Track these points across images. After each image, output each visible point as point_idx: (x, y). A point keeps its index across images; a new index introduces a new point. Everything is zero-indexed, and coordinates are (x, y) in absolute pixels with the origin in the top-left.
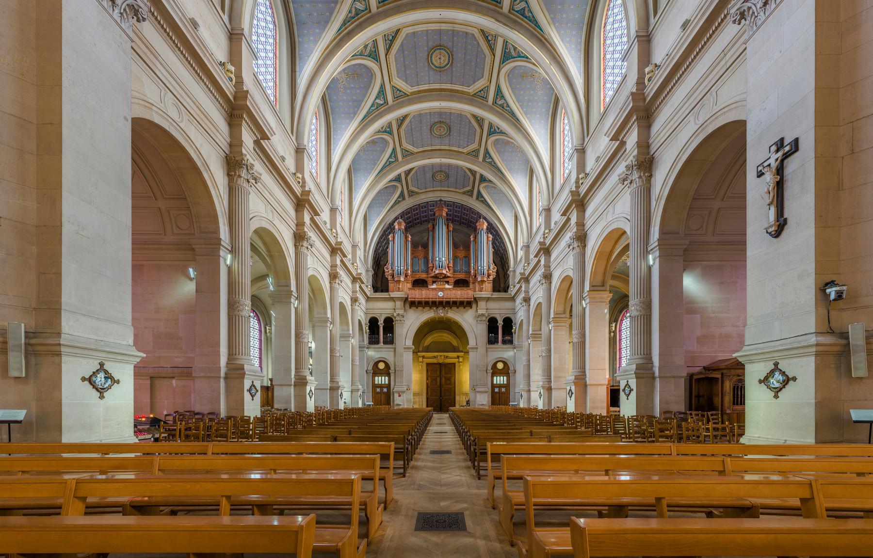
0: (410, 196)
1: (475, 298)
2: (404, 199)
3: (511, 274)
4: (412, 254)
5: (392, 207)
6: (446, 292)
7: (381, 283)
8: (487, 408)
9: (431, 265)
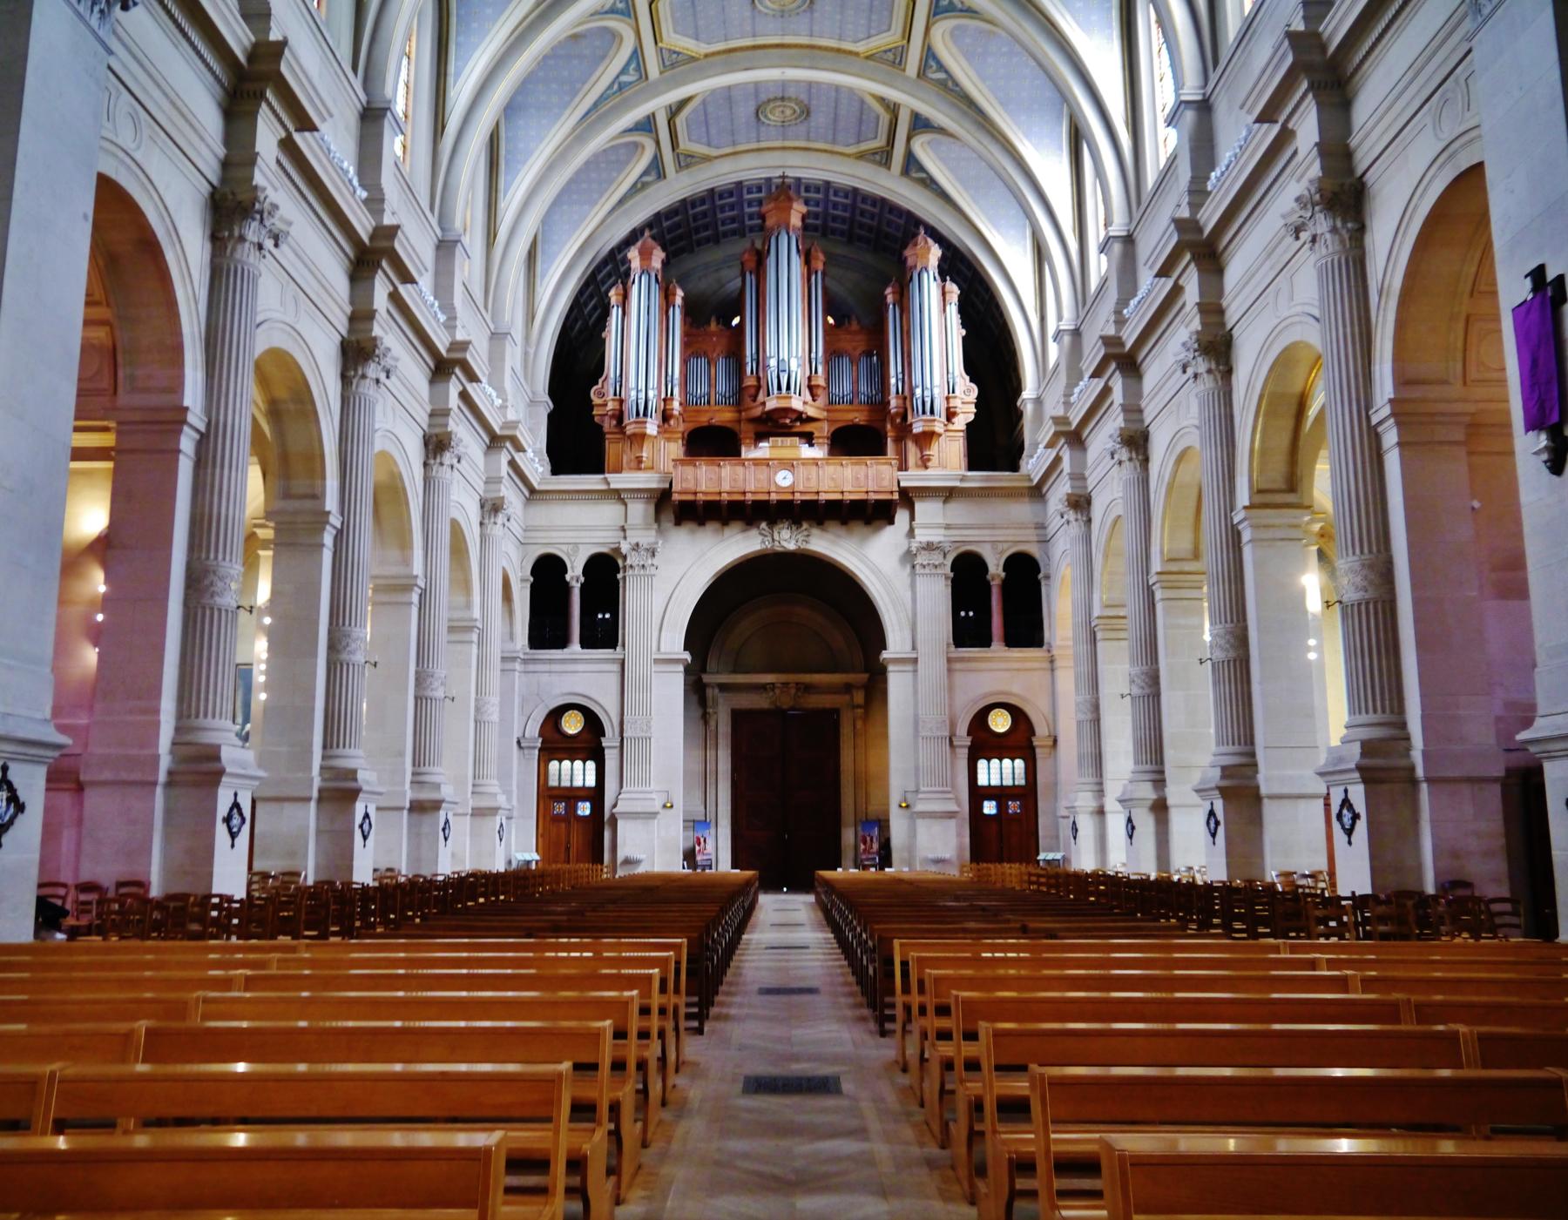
0: (680, 167)
1: (904, 492)
3: (1028, 410)
4: (686, 345)
5: (621, 202)
6: (801, 470)
7: (579, 439)
8: (953, 873)
9: (750, 381)
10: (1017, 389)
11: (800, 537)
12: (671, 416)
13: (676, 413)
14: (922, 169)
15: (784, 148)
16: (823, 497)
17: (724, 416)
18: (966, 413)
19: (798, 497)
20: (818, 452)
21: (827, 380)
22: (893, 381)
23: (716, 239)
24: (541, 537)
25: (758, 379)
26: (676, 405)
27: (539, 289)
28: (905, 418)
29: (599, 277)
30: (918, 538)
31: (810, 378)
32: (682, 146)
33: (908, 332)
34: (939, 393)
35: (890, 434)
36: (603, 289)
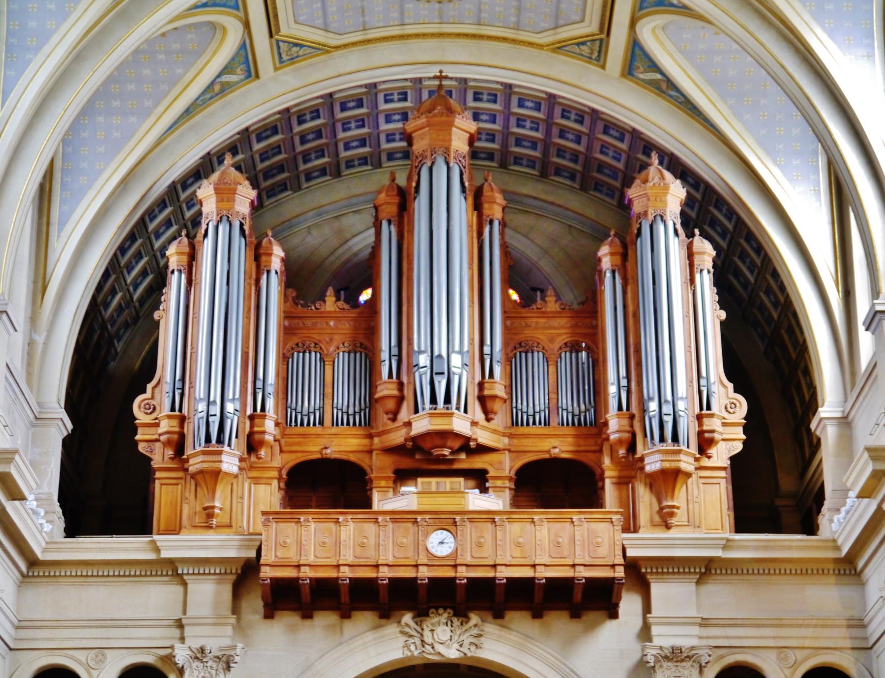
2: (252, 73)
4: (287, 332)
5: (189, 112)
6: (468, 530)
9: (386, 389)
10: (811, 404)
11: (467, 639)
12: (262, 443)
13: (269, 438)
14: (654, 66)
16: (504, 573)
17: (344, 444)
18: (730, 442)
20: (494, 502)
21: (509, 388)
22: (612, 389)
23: (335, 171)
24: (43, 637)
25: (401, 385)
26: (269, 425)
27: (56, 244)
28: (632, 447)
29: (152, 227)
30: (657, 641)
31: (481, 385)
32: (284, 30)
33: (636, 315)
34: (686, 408)
35: (610, 471)
36: (157, 245)
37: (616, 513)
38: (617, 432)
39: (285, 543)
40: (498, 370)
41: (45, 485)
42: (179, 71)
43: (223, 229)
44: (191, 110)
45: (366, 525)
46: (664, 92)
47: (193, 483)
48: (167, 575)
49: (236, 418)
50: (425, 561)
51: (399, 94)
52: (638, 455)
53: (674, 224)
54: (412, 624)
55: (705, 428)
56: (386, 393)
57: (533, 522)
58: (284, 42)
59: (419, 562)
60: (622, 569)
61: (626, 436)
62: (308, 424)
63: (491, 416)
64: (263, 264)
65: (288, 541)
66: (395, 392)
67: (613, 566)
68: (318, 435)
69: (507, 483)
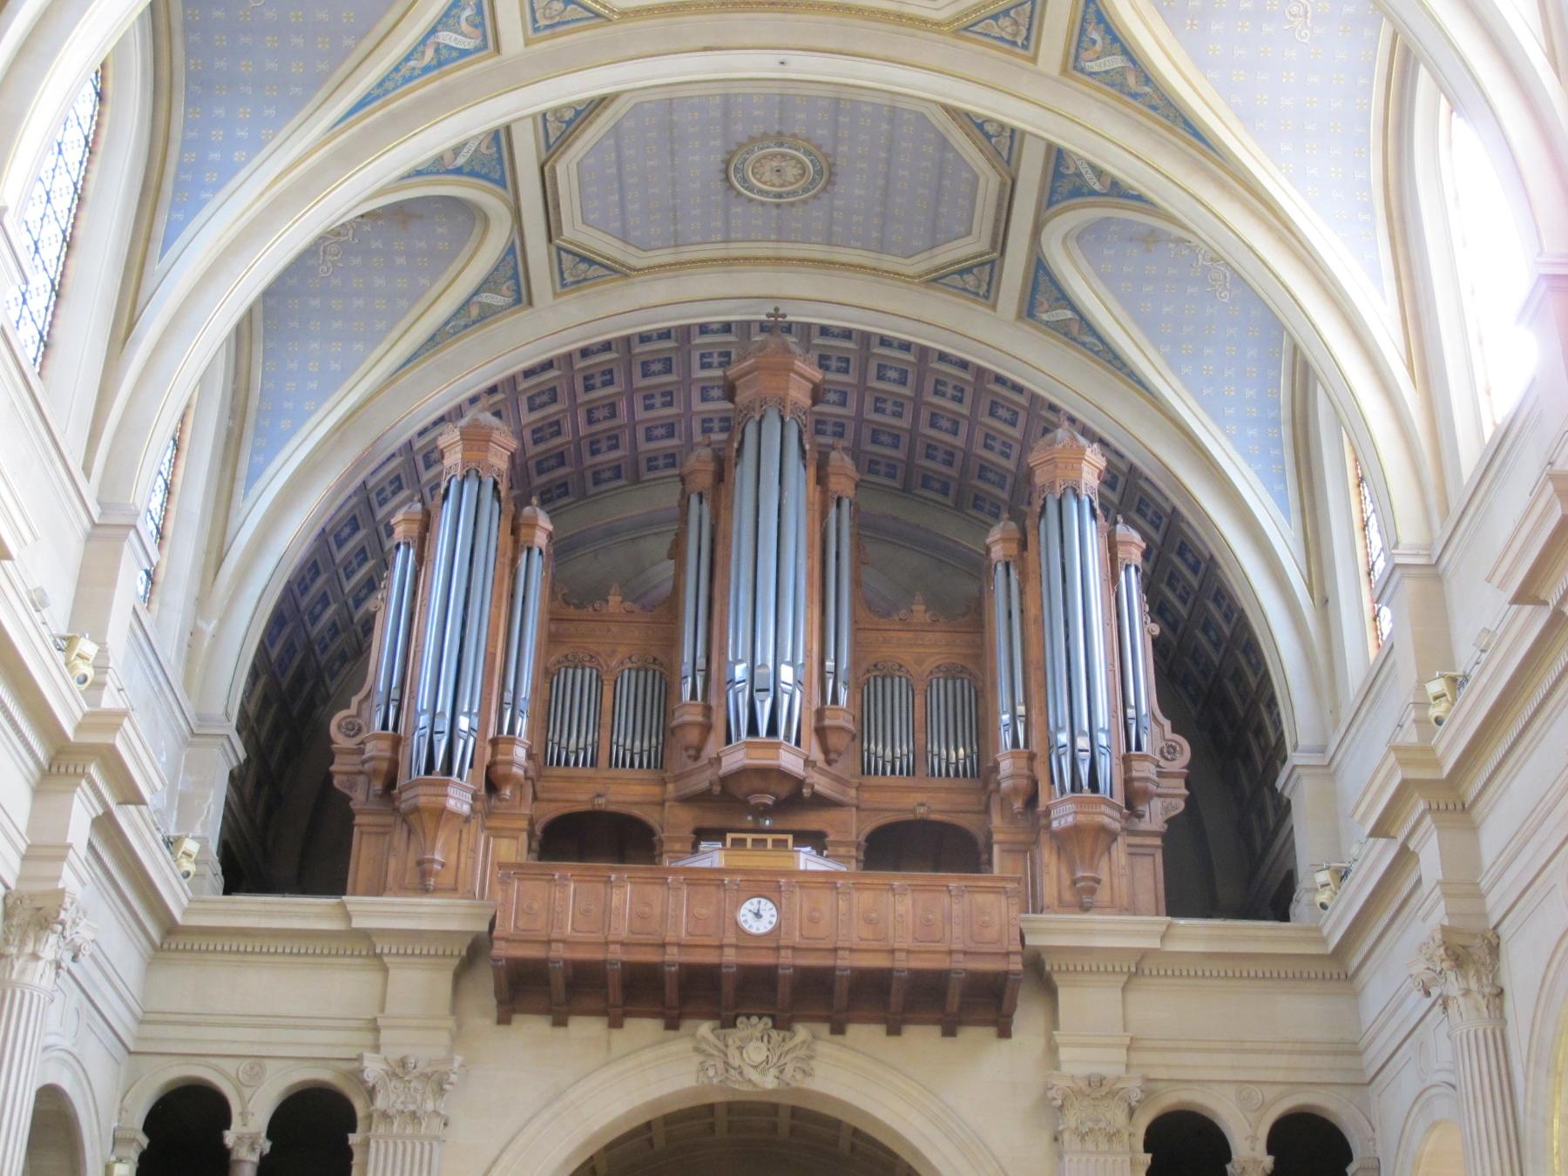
2: (522, 297)
4: (552, 638)
5: (434, 342)
12: (508, 778)
14: (1064, 299)
15: (778, 261)
16: (845, 961)
17: (626, 792)
19: (786, 958)
23: (632, 473)
25: (707, 710)
28: (1032, 800)
31: (820, 714)
32: (567, 232)
36: (381, 513)
37: (1012, 880)
38: (1012, 776)
39: (531, 908)
40: (843, 696)
41: (198, 826)
42: (423, 281)
43: (470, 488)
44: (438, 338)
45: (649, 888)
46: (1074, 340)
47: (405, 827)
48: (360, 956)
49: (471, 740)
50: (733, 941)
51: (720, 354)
52: (1041, 808)
53: (1091, 502)
54: (711, 1037)
55: (1135, 774)
56: (688, 718)
57: (892, 889)
58: (568, 252)
59: (726, 941)
60: (1018, 959)
61: (1023, 783)
62: (576, 763)
63: (833, 756)
64: (522, 539)
65: (536, 906)
66: (700, 719)
67: (1008, 954)
68: (589, 779)
69: (853, 852)
